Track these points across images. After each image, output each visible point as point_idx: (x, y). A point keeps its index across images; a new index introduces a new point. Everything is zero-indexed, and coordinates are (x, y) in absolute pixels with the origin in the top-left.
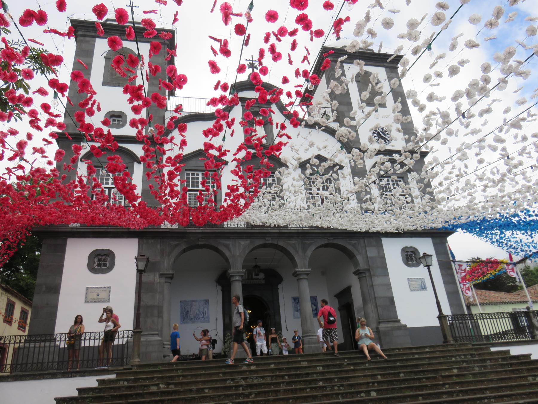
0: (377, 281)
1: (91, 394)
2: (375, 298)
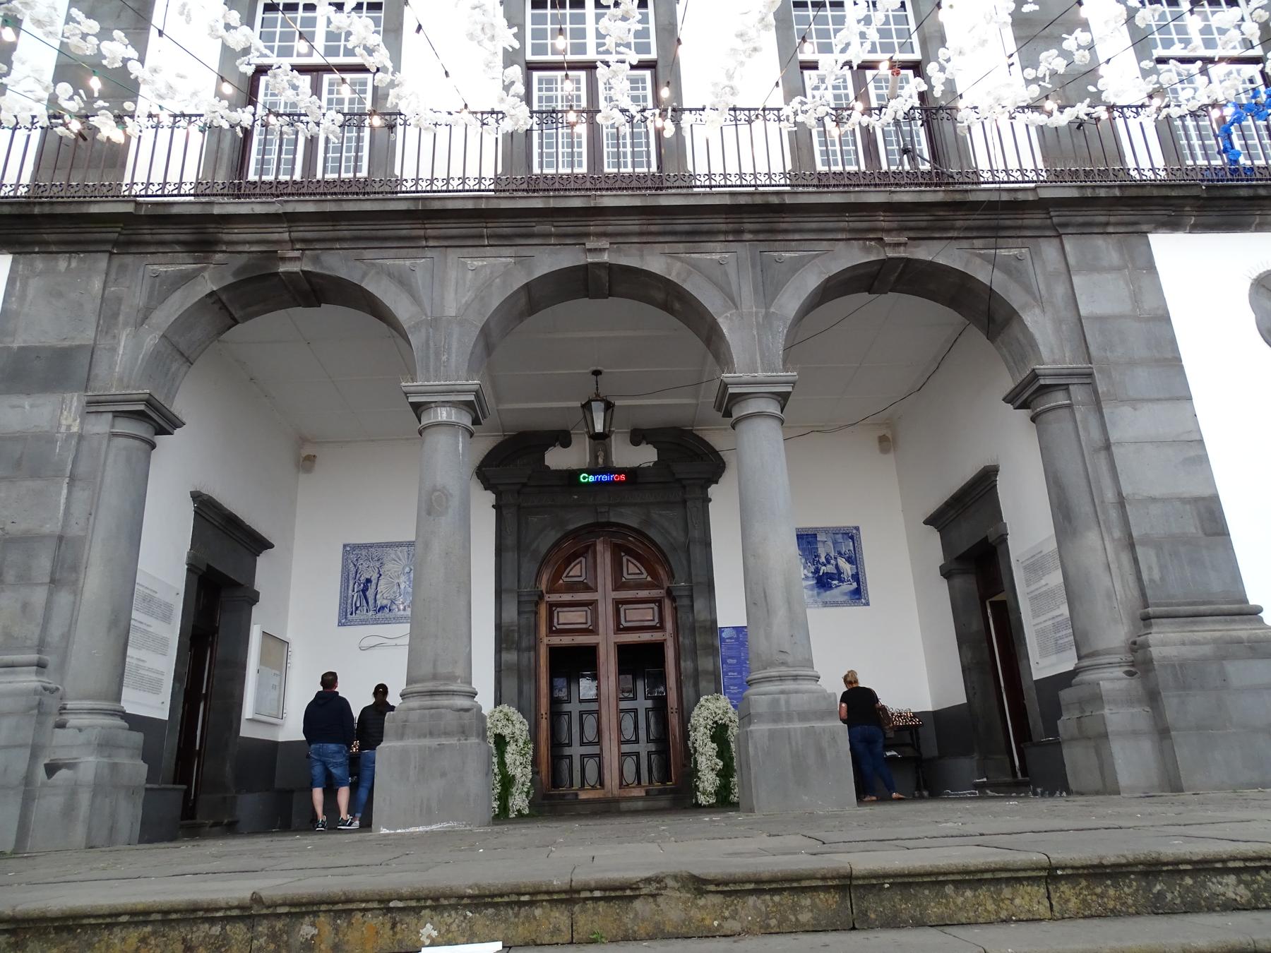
0: (1127, 424)
2: (1121, 502)
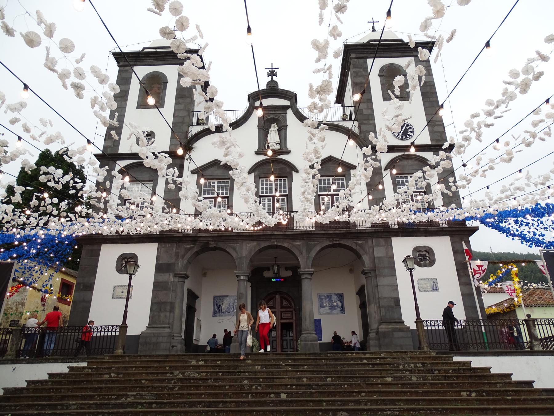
0: (383, 281)
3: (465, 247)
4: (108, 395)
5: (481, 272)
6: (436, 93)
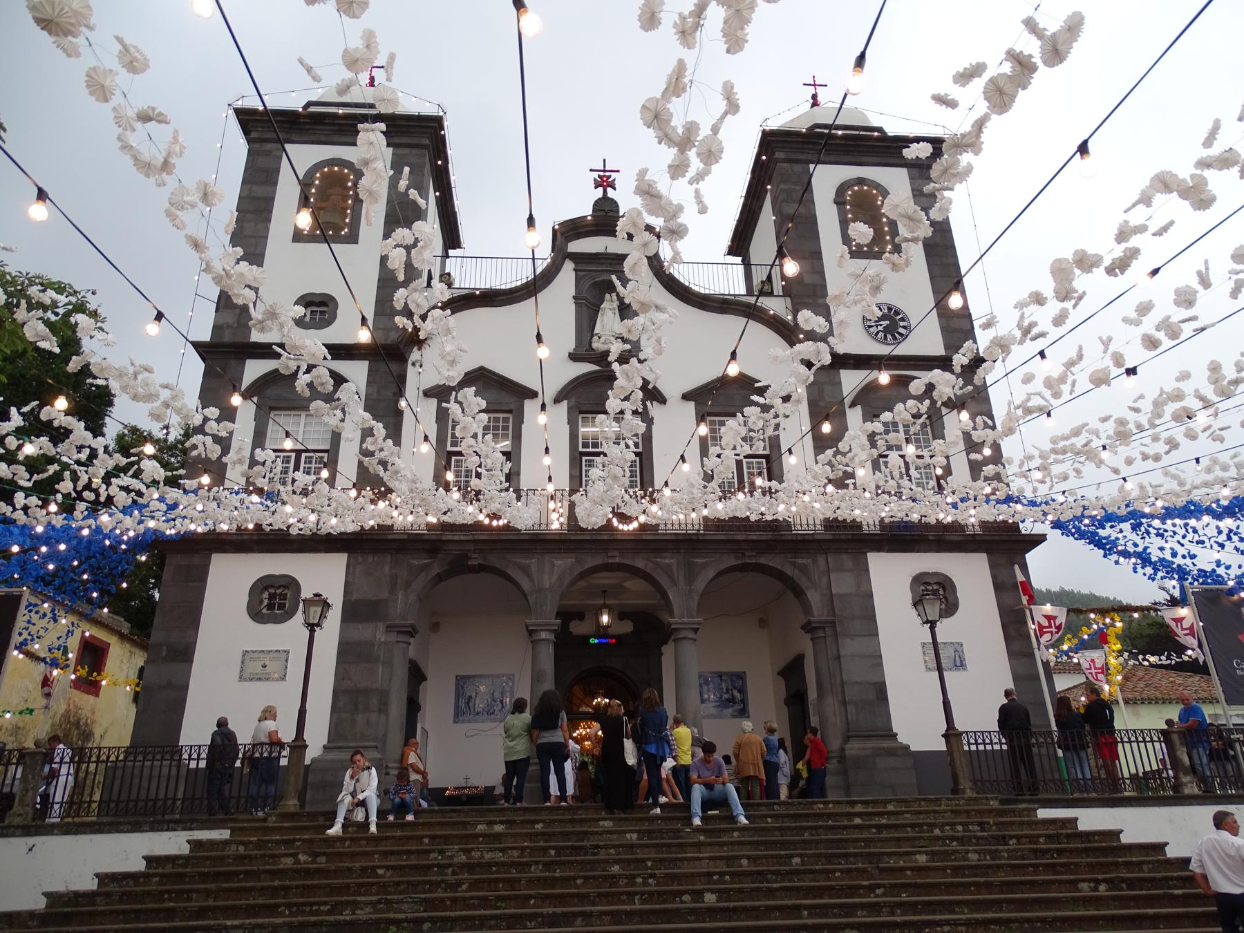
0: (850, 647)
1: (169, 869)
2: (843, 684)
3: (1020, 577)
4: (311, 904)
5: (1054, 630)
6: (953, 247)
